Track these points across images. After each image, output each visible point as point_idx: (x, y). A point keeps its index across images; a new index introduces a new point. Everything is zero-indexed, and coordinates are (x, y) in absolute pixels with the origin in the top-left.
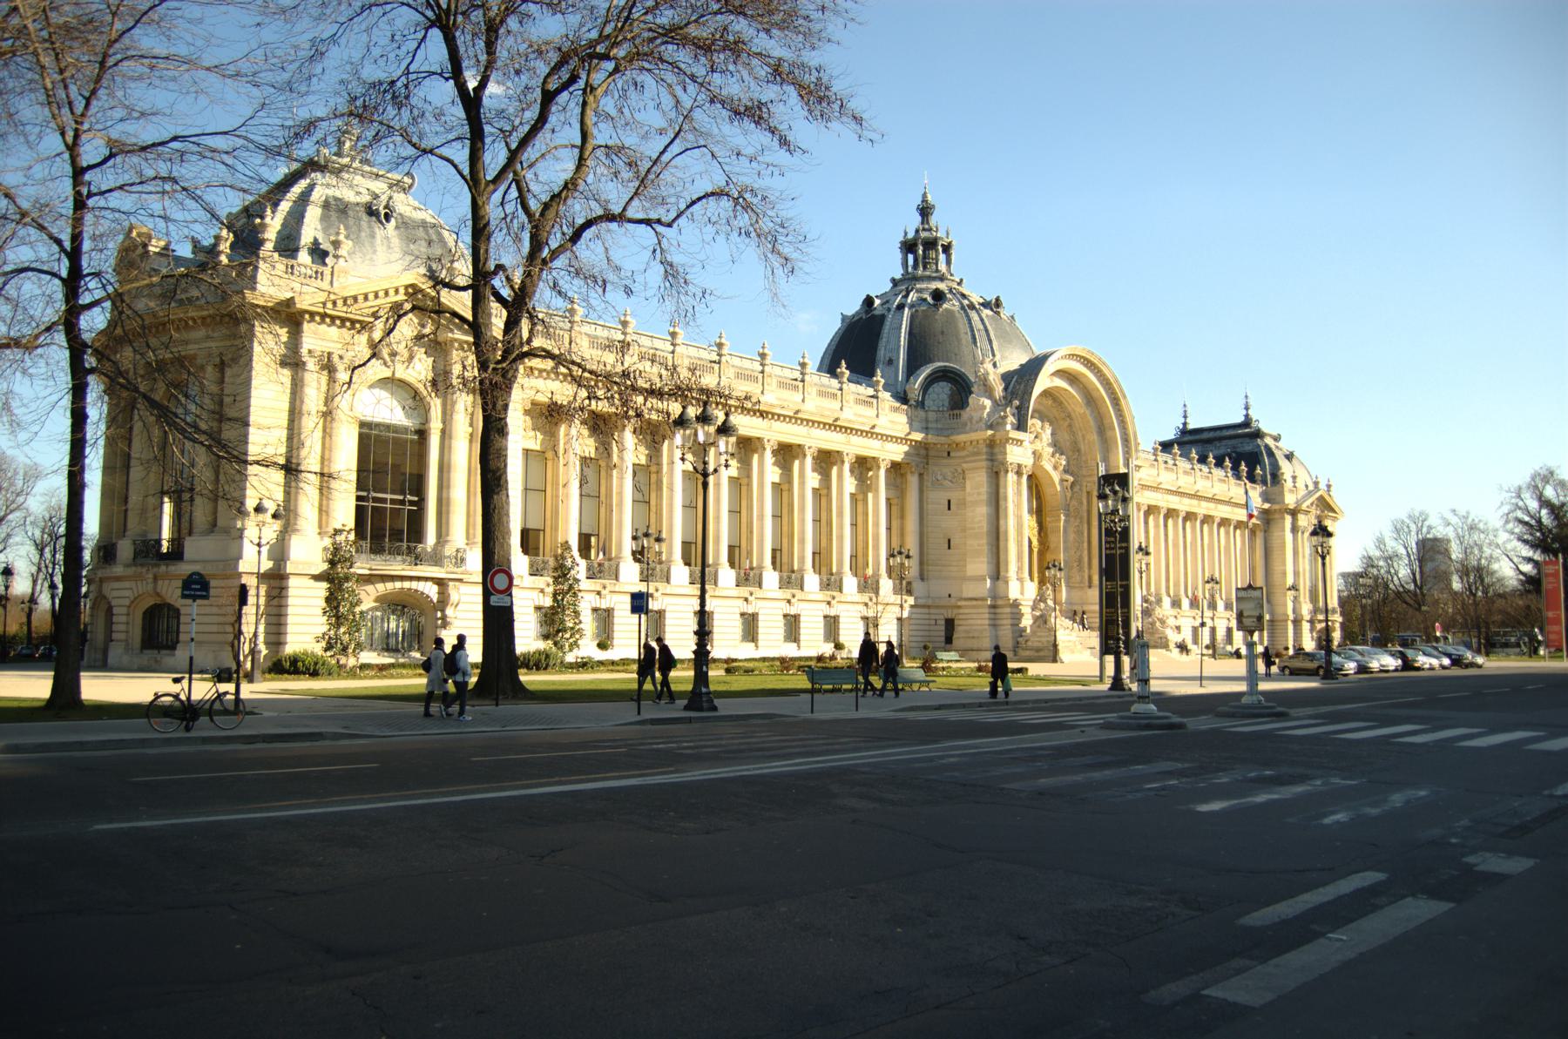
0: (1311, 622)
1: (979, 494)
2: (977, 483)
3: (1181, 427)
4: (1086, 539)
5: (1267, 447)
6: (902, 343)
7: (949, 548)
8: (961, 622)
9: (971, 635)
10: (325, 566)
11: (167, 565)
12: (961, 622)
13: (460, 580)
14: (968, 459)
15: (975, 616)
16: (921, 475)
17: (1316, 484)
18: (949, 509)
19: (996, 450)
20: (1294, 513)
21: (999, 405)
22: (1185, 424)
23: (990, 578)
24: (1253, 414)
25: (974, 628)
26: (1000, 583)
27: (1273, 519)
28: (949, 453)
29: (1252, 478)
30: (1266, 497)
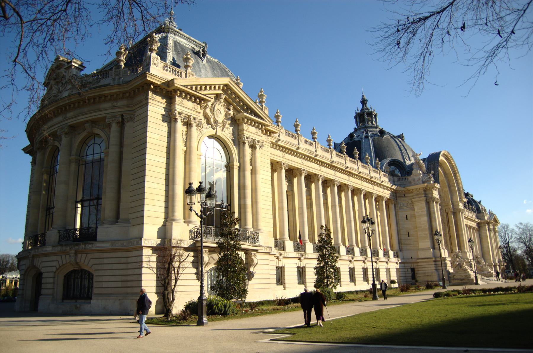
0: (499, 266)
1: (422, 211)
2: (420, 207)
6: (372, 151)
7: (409, 236)
8: (419, 269)
9: (427, 275)
10: (191, 242)
11: (85, 244)
13: (256, 251)
14: (414, 197)
15: (427, 266)
16: (395, 205)
18: (407, 219)
19: (427, 192)
20: (488, 223)
21: (424, 173)
23: (432, 249)
25: (427, 271)
28: (404, 195)
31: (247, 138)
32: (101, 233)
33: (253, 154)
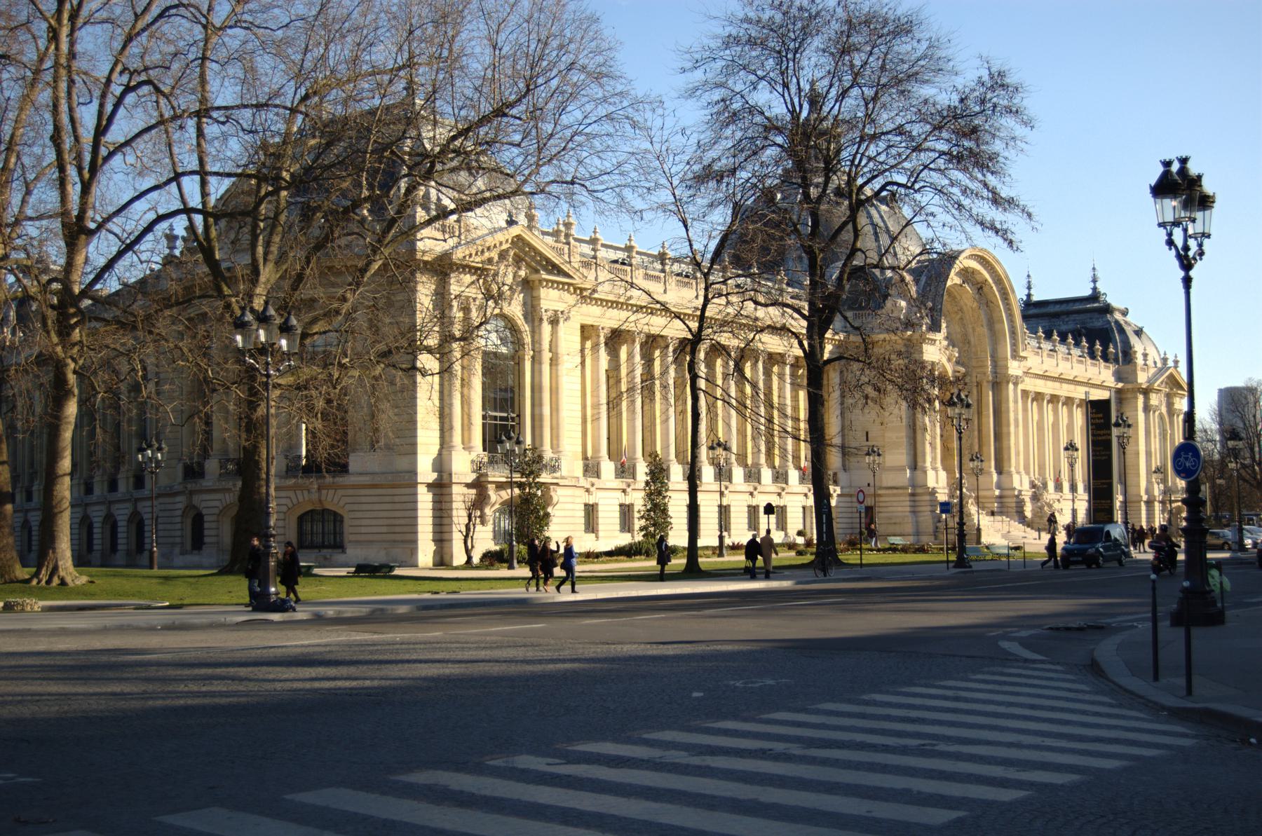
3: (1025, 298)
4: (976, 427)
5: (1117, 322)
8: (881, 510)
9: (893, 521)
10: (474, 476)
11: (334, 477)
12: (881, 510)
13: (557, 484)
15: (895, 504)
16: (841, 372)
17: (1165, 360)
20: (1146, 392)
22: (1029, 296)
23: (910, 469)
24: (1101, 287)
26: (918, 473)
27: (1126, 399)
29: (1105, 358)
30: (1119, 377)
31: (546, 311)
32: (354, 462)
33: (554, 333)
